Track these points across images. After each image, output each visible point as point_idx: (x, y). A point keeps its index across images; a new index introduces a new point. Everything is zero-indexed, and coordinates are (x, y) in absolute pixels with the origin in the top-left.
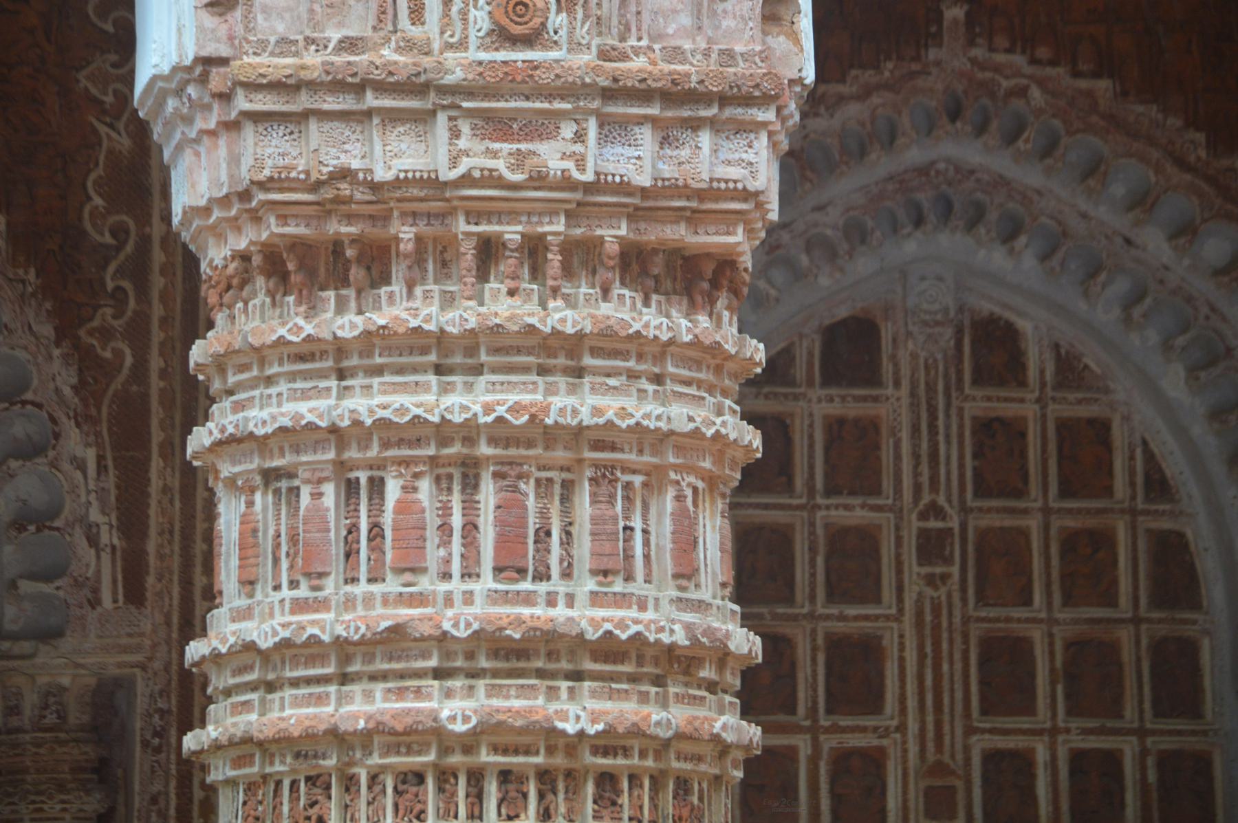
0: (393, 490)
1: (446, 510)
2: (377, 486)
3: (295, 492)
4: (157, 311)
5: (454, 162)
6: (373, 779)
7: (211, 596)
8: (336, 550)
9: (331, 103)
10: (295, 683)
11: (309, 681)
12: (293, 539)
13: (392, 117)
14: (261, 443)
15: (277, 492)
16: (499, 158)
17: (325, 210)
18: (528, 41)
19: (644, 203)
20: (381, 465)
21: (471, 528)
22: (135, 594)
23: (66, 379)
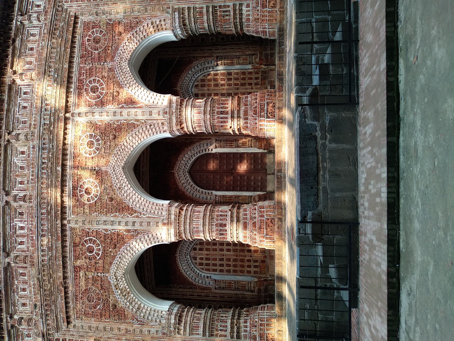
7: (203, 133)
13: (172, 121)
19: (177, 105)
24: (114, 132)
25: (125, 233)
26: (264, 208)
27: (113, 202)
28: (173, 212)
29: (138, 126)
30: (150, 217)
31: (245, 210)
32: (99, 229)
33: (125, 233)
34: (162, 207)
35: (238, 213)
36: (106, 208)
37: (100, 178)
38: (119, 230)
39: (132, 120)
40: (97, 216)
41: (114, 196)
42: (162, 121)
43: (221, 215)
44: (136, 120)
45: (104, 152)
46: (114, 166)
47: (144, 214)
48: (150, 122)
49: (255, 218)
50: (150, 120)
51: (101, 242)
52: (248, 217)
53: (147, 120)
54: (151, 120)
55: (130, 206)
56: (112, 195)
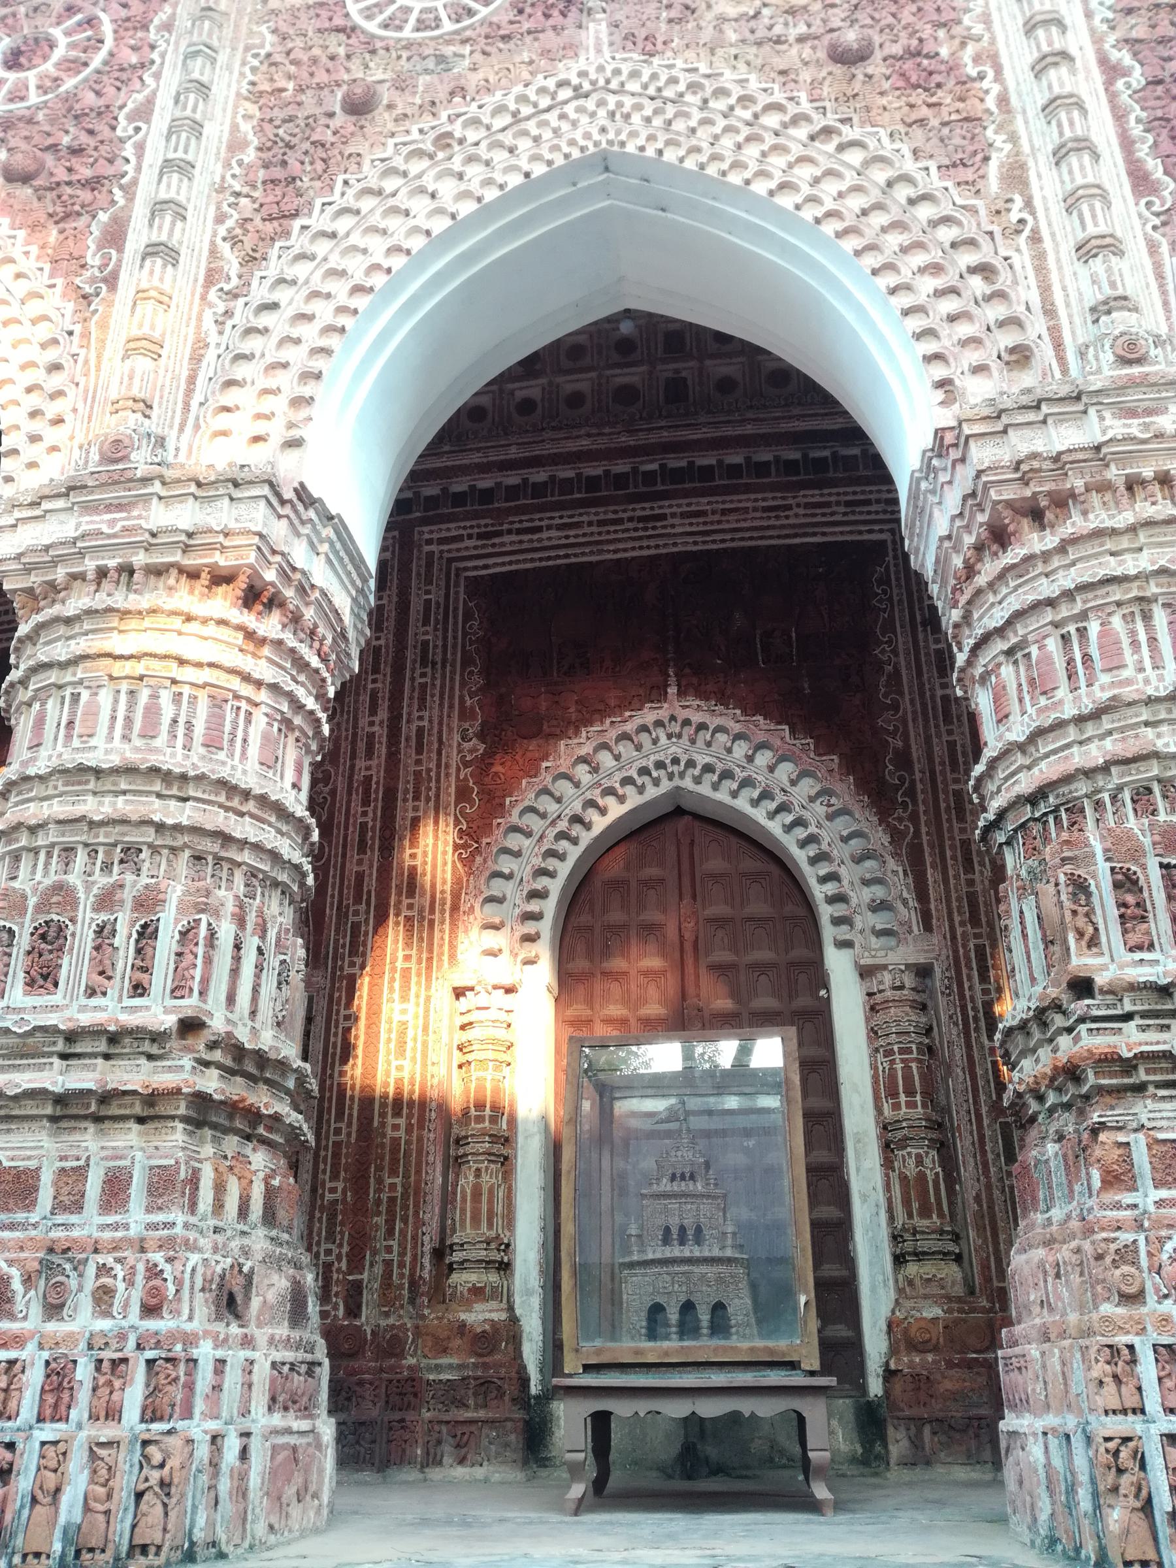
0: (1094, 628)
1: (1133, 633)
2: (1082, 632)
3: (1028, 656)
4: (922, 808)
5: (1104, 432)
6: (1114, 798)
8: (1062, 675)
9: (1020, 419)
10: (1047, 755)
11: (1054, 752)
12: (1032, 682)
13: (1061, 418)
14: (1000, 632)
15: (1016, 662)
16: (1134, 427)
17: (1025, 481)
18: (1139, 361)
20: (1083, 616)
21: (1152, 640)
22: (928, 927)
23: (886, 840)
24: (897, 49)
25: (103, 217)
26: (151, 1414)
27: (340, 119)
28: (221, 515)
29: (972, 186)
30: (196, 359)
31: (166, 1185)
32: (157, 76)
33: (103, 217)
34: (276, 440)
35: (150, 1109)
36: (300, 90)
37: (526, 25)
38: (135, 182)
39: (1013, 138)
40: (247, 49)
41: (383, 118)
42: (1045, 352)
43: (147, 933)
44: (1023, 166)
45: (723, 19)
46: (621, 90)
47: (228, 313)
48: (1023, 260)
49: (54, 1310)
50: (1040, 260)
51: (69, 99)
52: (89, 1223)
53: (1036, 238)
54: (1041, 269)
55: (297, 224)
56: (390, 107)
